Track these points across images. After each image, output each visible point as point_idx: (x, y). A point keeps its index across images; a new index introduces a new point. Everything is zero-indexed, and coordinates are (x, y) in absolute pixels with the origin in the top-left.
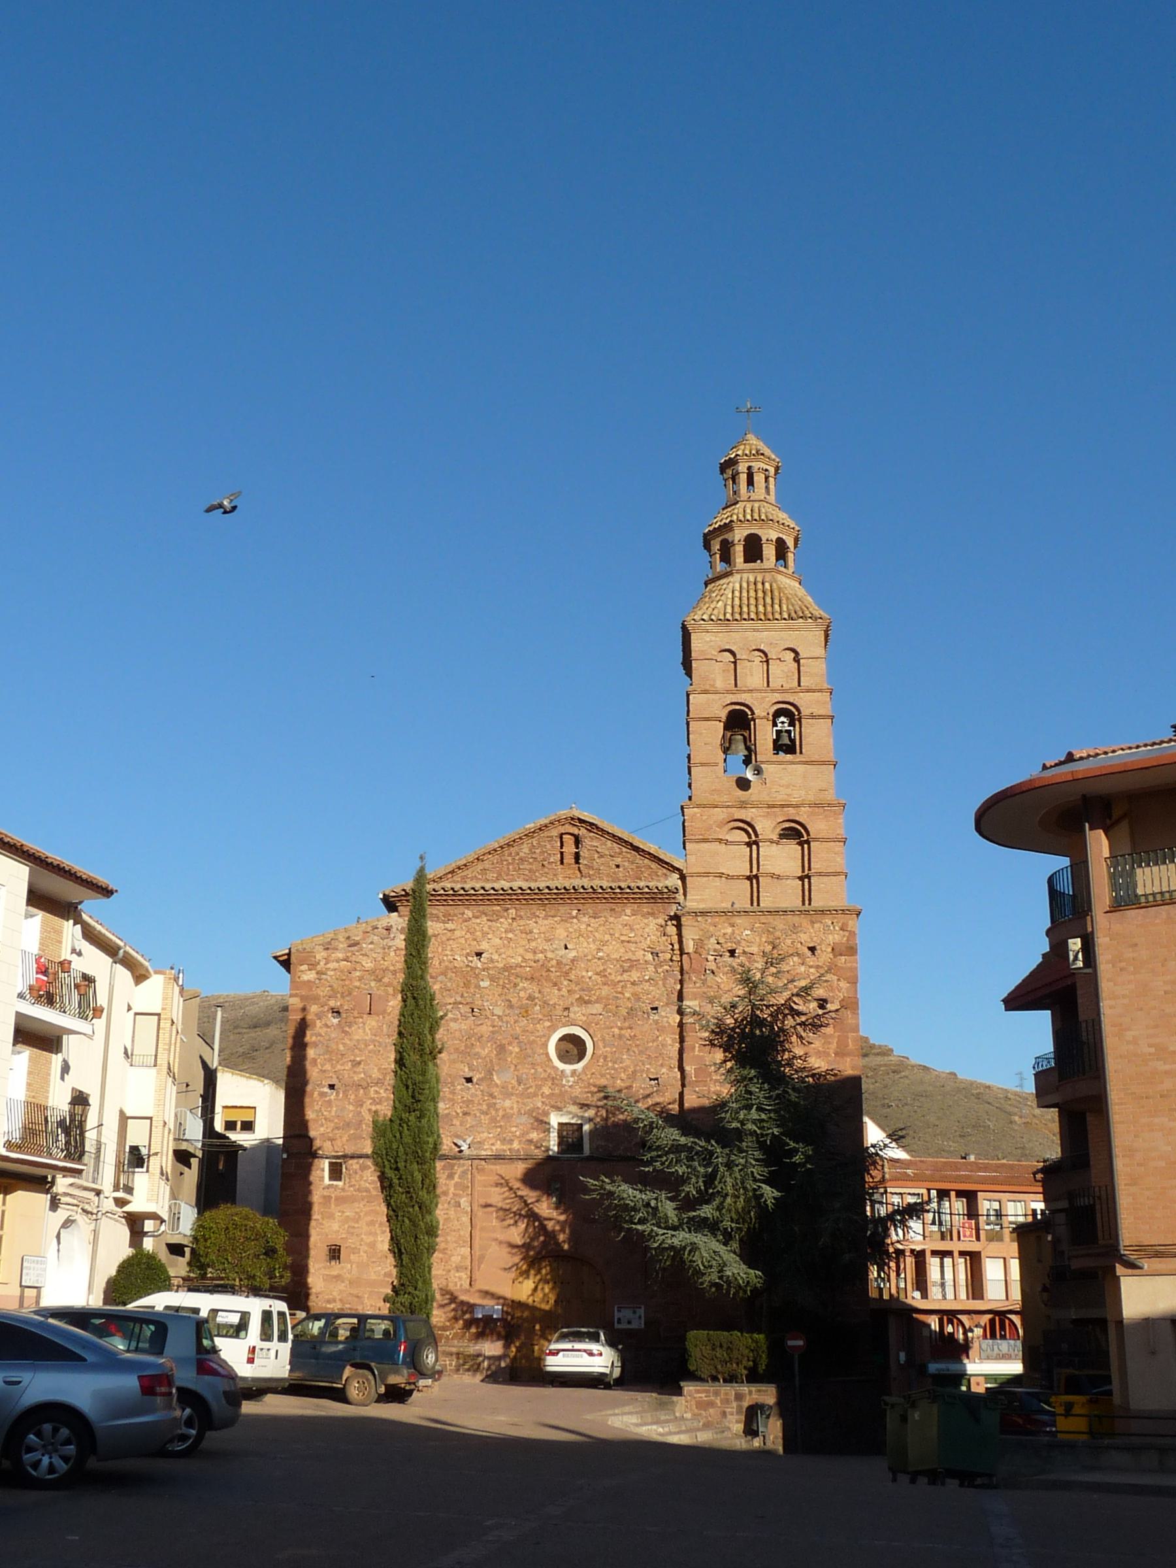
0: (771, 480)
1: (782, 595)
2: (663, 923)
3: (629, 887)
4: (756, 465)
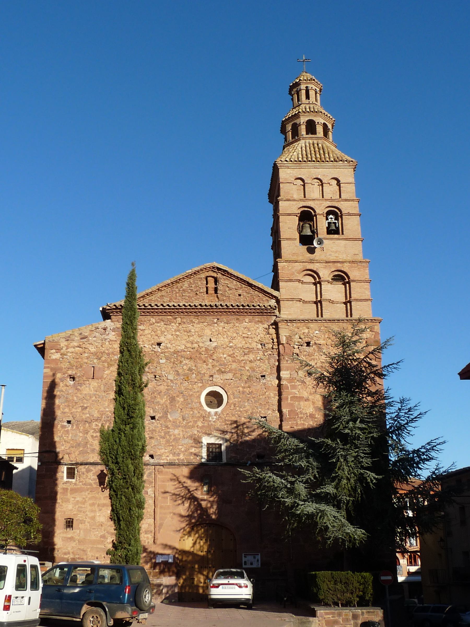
0: (318, 95)
1: (329, 150)
2: (267, 327)
3: (248, 305)
4: (310, 86)
